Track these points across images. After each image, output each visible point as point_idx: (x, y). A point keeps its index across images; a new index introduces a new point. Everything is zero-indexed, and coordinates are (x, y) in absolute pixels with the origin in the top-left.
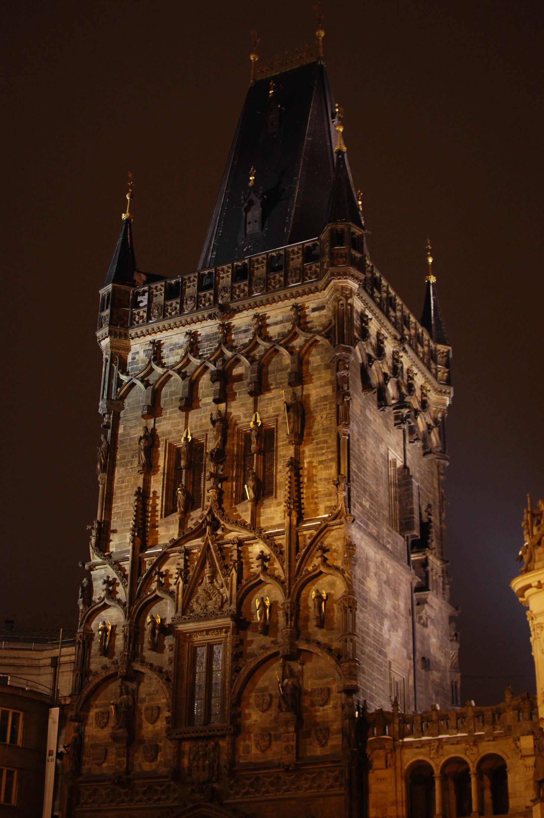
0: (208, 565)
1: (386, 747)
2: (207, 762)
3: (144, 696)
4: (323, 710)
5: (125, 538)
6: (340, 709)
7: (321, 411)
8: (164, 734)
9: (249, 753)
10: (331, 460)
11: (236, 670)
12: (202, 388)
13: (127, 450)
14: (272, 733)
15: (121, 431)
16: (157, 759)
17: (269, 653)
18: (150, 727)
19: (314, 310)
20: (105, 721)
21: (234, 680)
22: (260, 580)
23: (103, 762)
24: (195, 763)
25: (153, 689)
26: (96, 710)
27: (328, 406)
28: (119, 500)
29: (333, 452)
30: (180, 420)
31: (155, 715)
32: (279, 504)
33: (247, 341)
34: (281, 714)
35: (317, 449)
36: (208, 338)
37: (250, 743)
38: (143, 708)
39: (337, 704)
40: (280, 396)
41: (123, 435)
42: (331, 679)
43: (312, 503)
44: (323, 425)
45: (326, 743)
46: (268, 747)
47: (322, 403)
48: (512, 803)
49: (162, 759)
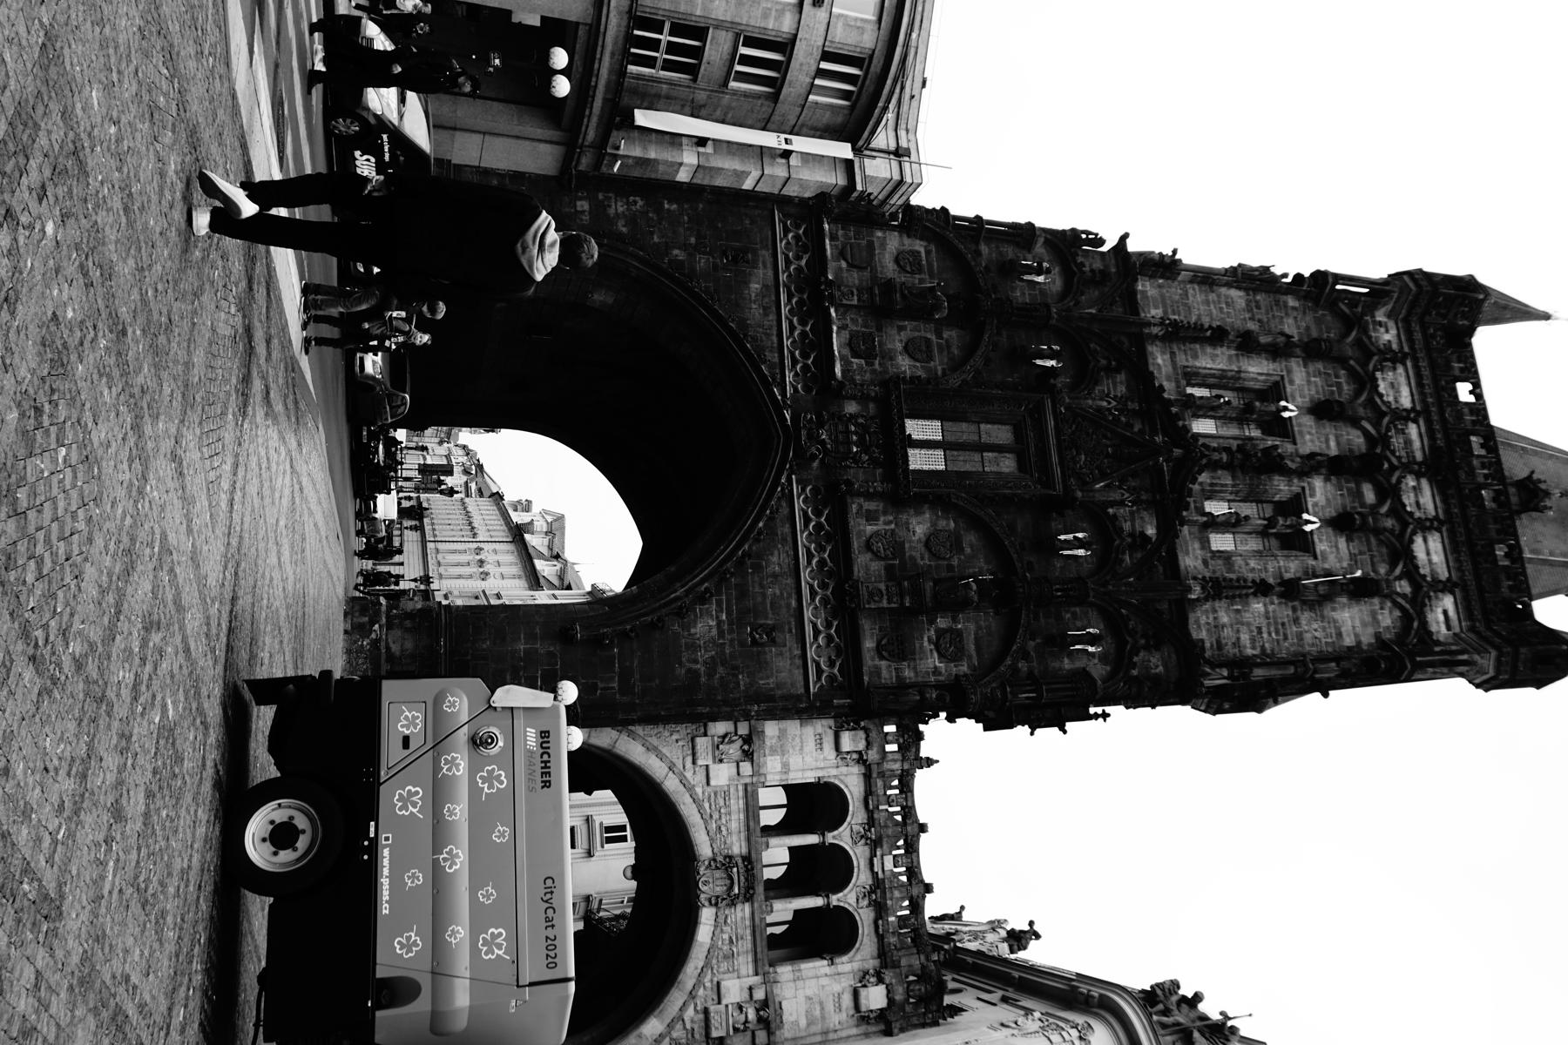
1: (870, 752)
3: (945, 336)
7: (1324, 629)
8: (892, 370)
9: (867, 520)
10: (1263, 647)
12: (1348, 434)
13: (1267, 313)
15: (1292, 302)
17: (1015, 556)
18: (899, 346)
19: (1445, 612)
20: (908, 269)
23: (848, 262)
24: (853, 428)
25: (956, 352)
26: (922, 250)
27: (1329, 640)
28: (1203, 297)
29: (1272, 650)
30: (1307, 400)
32: (1205, 562)
33: (1408, 509)
34: (931, 584)
35: (1276, 623)
36: (1408, 442)
38: (929, 336)
40: (1340, 560)
41: (1286, 305)
43: (1208, 618)
44: (1306, 632)
45: (882, 658)
46: (877, 556)
47: (1333, 631)
48: (785, 971)
49: (855, 367)
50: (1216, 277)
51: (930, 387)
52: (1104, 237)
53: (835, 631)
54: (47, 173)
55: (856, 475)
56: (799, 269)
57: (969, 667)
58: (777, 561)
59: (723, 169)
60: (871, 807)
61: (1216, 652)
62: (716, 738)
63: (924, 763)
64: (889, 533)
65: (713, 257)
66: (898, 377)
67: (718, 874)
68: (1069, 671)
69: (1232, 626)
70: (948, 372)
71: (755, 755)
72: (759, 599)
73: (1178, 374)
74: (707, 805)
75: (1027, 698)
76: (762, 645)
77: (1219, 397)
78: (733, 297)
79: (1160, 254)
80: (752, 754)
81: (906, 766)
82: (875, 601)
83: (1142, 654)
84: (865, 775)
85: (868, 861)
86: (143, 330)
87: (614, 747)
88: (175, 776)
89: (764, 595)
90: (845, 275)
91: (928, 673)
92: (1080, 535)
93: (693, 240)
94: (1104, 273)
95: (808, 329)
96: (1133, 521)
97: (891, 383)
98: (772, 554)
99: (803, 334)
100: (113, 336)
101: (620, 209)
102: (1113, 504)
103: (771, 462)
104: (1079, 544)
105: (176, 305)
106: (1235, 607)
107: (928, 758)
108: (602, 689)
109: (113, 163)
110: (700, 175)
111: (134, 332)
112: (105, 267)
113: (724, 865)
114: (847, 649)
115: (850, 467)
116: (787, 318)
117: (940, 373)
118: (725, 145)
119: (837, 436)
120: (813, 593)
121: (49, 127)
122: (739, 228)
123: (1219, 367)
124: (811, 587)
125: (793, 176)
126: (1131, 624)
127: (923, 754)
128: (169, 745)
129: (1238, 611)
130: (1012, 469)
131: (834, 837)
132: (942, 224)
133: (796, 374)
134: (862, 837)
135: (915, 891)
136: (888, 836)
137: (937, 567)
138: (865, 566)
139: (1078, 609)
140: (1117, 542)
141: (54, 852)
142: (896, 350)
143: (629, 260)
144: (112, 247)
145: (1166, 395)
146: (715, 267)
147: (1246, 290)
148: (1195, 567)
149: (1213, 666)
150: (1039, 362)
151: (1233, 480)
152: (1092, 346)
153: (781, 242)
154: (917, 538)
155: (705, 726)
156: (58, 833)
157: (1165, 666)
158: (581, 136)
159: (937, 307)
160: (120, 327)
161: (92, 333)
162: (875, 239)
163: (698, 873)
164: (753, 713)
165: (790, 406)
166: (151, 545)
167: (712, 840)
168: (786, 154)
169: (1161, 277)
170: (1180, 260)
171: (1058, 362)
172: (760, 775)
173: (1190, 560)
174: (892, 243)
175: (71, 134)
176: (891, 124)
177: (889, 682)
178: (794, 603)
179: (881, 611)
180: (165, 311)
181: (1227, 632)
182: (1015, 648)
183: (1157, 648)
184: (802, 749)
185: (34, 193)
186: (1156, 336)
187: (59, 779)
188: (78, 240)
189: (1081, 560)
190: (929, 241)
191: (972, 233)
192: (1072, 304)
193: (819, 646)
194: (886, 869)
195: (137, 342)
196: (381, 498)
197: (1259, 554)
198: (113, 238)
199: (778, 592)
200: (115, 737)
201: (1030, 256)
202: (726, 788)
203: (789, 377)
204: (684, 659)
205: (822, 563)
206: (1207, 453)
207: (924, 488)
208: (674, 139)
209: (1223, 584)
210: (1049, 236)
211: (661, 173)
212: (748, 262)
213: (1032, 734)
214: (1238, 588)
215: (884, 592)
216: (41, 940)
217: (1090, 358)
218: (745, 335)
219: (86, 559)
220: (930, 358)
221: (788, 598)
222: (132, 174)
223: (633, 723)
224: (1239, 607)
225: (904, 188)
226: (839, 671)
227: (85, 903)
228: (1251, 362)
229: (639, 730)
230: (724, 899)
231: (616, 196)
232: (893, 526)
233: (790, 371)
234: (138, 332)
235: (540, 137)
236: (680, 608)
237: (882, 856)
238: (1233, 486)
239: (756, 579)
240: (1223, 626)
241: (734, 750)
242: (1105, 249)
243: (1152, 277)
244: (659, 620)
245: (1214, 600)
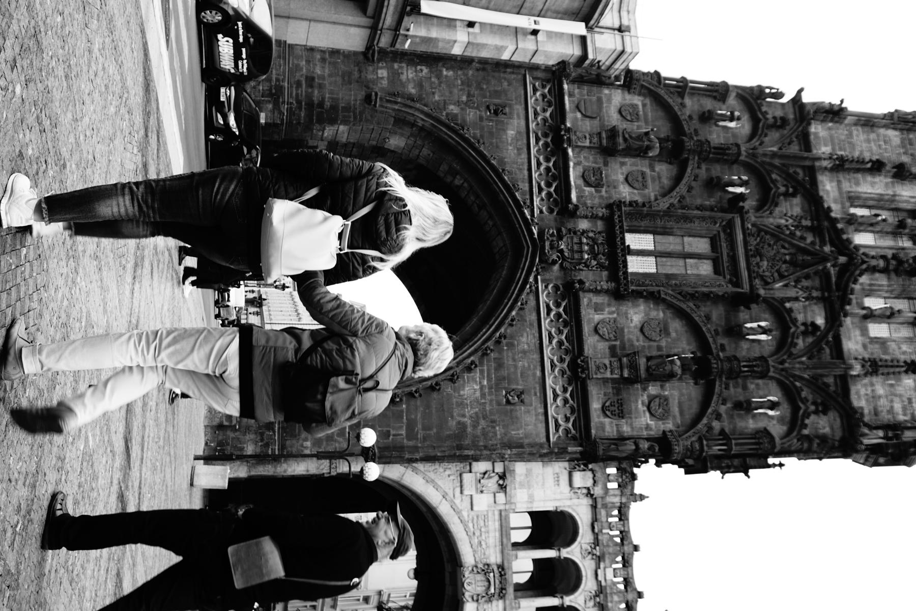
0: (806, 257)
1: (596, 488)
2: (586, 256)
3: (657, 168)
4: (644, 411)
5: (826, 145)
6: (645, 433)
8: (615, 197)
9: (595, 311)
11: (693, 296)
14: (618, 343)
16: (585, 186)
17: (711, 340)
18: (621, 178)
20: (629, 118)
21: (680, 294)
22: (791, 328)
23: (582, 113)
24: (585, 240)
26: (640, 104)
31: (636, 185)
32: (865, 346)
34: (645, 360)
37: (606, 312)
38: (644, 169)
39: (651, 429)
42: (679, 422)
43: (866, 390)
45: (607, 416)
49: (587, 193)
50: (876, 120)
51: (645, 209)
52: (784, 91)
53: (571, 395)
54: (17, 50)
55: (588, 276)
56: (545, 120)
57: (674, 425)
58: (526, 340)
59: (487, 45)
60: (596, 530)
61: (874, 417)
62: (478, 475)
63: (638, 498)
64: (612, 321)
65: (480, 111)
66: (620, 202)
67: (480, 577)
68: (752, 429)
69: (887, 396)
70: (659, 197)
71: (508, 488)
72: (512, 370)
73: (843, 198)
74: (471, 525)
75: (720, 450)
76: (514, 404)
77: (877, 215)
78: (494, 141)
79: (830, 103)
80: (505, 487)
81: (624, 500)
82: (600, 372)
83: (813, 417)
84: (592, 505)
85: (594, 572)
86: (77, 165)
87: (402, 479)
88: (93, 489)
89: (516, 367)
90: (580, 123)
91: (641, 428)
92: (763, 324)
93: (464, 98)
94: (782, 119)
95: (551, 164)
96: (805, 313)
97: (614, 207)
98: (522, 336)
99: (548, 169)
100: (57, 168)
101: (410, 76)
102: (789, 299)
103: (522, 266)
104: (764, 331)
105: (99, 147)
106: (890, 382)
107: (641, 495)
108: (394, 435)
109: (59, 43)
110: (469, 49)
111: (71, 166)
112: (52, 119)
113: (483, 570)
114: (581, 409)
115: (582, 270)
116: (535, 156)
117: (653, 198)
118: (488, 27)
119: (572, 247)
120: (553, 366)
121: (19, 17)
122: (499, 88)
123: (879, 191)
124: (552, 361)
125: (540, 48)
126: (804, 394)
127: (638, 490)
128: (89, 466)
129: (892, 385)
130: (708, 272)
131: (568, 553)
132: (656, 83)
133: (542, 200)
134: (589, 553)
135: (631, 596)
136: (610, 554)
137: (649, 347)
138: (594, 347)
139: (760, 382)
140: (793, 330)
141: (14, 540)
142: (617, 181)
143: (416, 113)
144: (57, 104)
145: (833, 215)
146: (481, 119)
147: (901, 130)
148: (856, 350)
149: (871, 428)
150: (731, 189)
151: (889, 279)
152: (774, 176)
153: (531, 98)
154: (632, 325)
155: (470, 465)
156: (16, 526)
157: (832, 428)
158: (381, 21)
159: (649, 148)
160: (62, 162)
161: (45, 166)
162: (603, 96)
163: (464, 576)
164: (507, 456)
165: (537, 224)
166: (79, 320)
167: (474, 551)
168: (535, 32)
169: (832, 121)
170: (846, 108)
171: (746, 189)
172: (511, 503)
173: (852, 344)
174: (616, 98)
175: (33, 22)
176: (616, 7)
177: (611, 435)
178: (538, 373)
179: (605, 381)
180: (91, 151)
181: (883, 402)
182: (710, 410)
183: (825, 412)
184: (543, 484)
185: (8, 64)
186: (826, 168)
187: (18, 487)
188: (36, 99)
189: (763, 343)
190: (644, 96)
191: (679, 90)
192: (757, 143)
193: (557, 406)
194: (607, 578)
195: (73, 173)
196: (233, 291)
197: (910, 340)
198: (58, 97)
199: (526, 364)
200: (54, 458)
201: (724, 107)
202: (485, 513)
203: (537, 201)
204: (455, 414)
205: (560, 343)
206: (866, 260)
207: (639, 285)
208: (450, 23)
209: (880, 363)
210: (740, 92)
211: (440, 49)
212: (505, 114)
213: (723, 478)
214: (892, 366)
215: (608, 366)
216: (5, 603)
217: (772, 185)
218: (503, 170)
219: (38, 330)
220: (645, 186)
221: (534, 369)
222: (71, 51)
223: (416, 461)
224: (893, 382)
225: (624, 57)
226: (573, 425)
227: (33, 578)
228: (905, 188)
229: (420, 466)
230: (483, 597)
231: (407, 66)
232: (615, 315)
233: (537, 197)
234: (74, 166)
235: (351, 23)
236: (453, 375)
237: (605, 568)
238: (889, 286)
239: (510, 354)
240: (880, 397)
241: (492, 483)
242: (784, 100)
243: (823, 121)
244: (437, 384)
245: (871, 374)
